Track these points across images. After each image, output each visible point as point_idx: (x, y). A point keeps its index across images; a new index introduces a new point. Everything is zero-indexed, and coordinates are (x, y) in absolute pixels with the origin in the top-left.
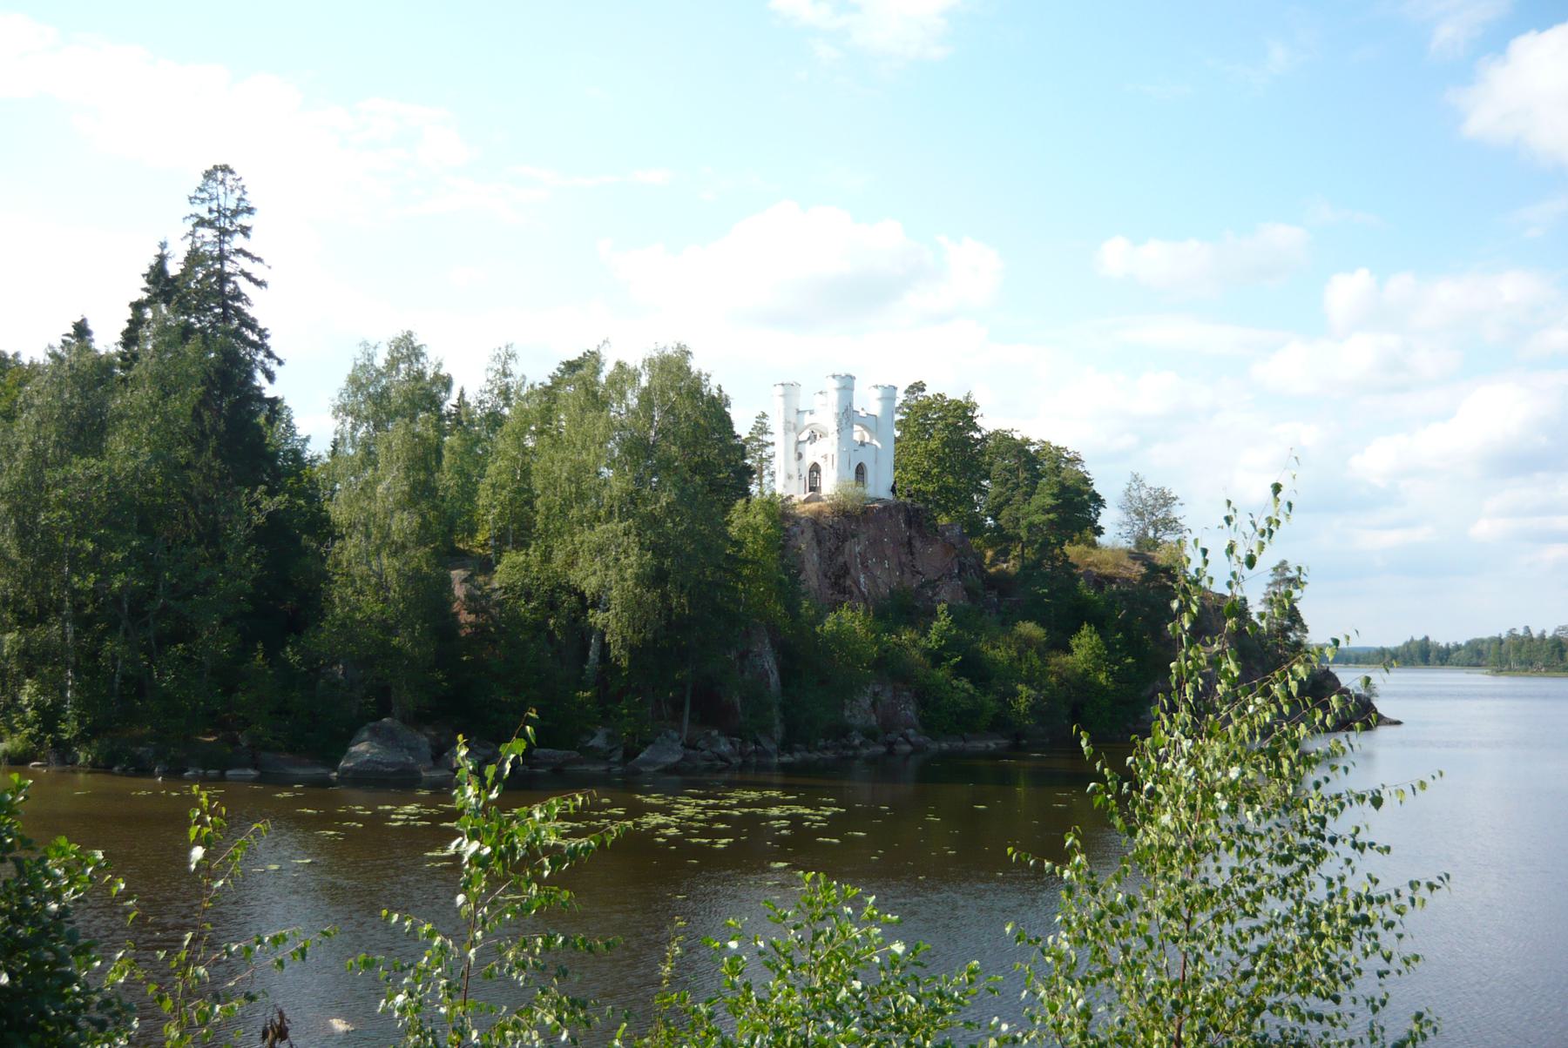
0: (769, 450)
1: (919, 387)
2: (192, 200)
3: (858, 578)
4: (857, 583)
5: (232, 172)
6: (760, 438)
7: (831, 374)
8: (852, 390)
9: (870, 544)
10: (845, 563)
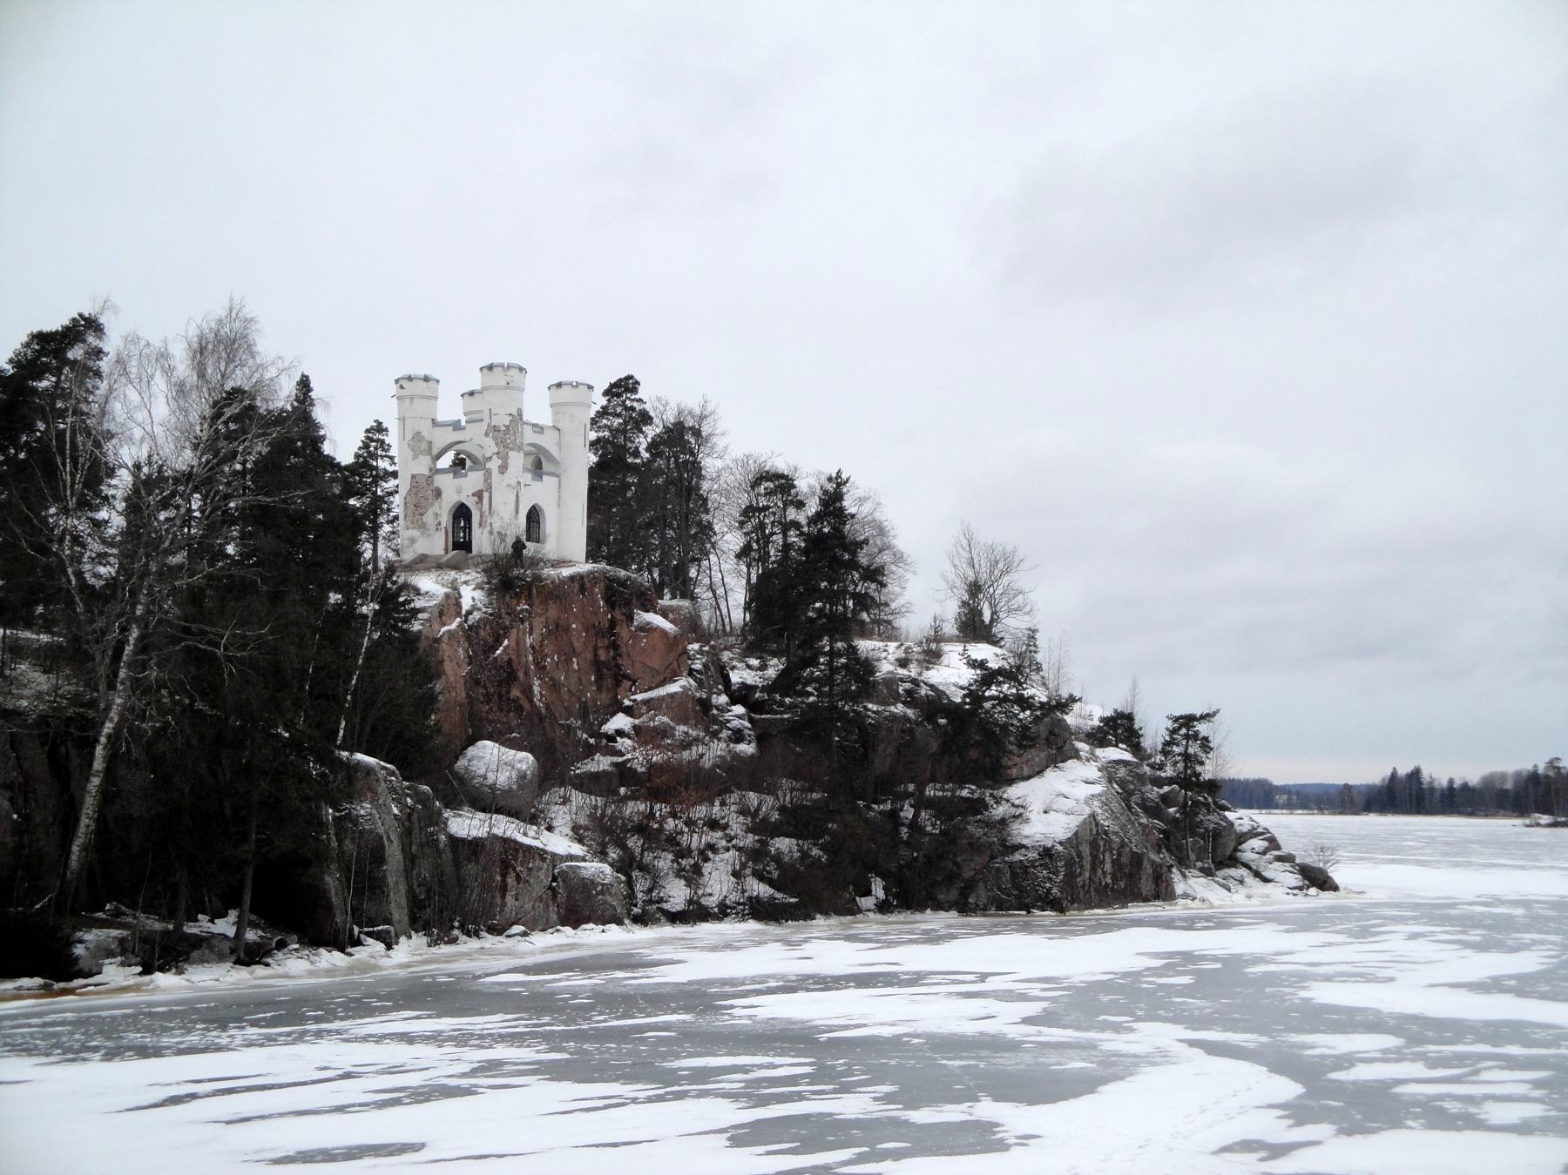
0: (390, 484)
1: (624, 387)
3: (531, 687)
4: (528, 691)
6: (375, 463)
7: (488, 363)
8: (523, 390)
9: (549, 632)
10: (510, 660)
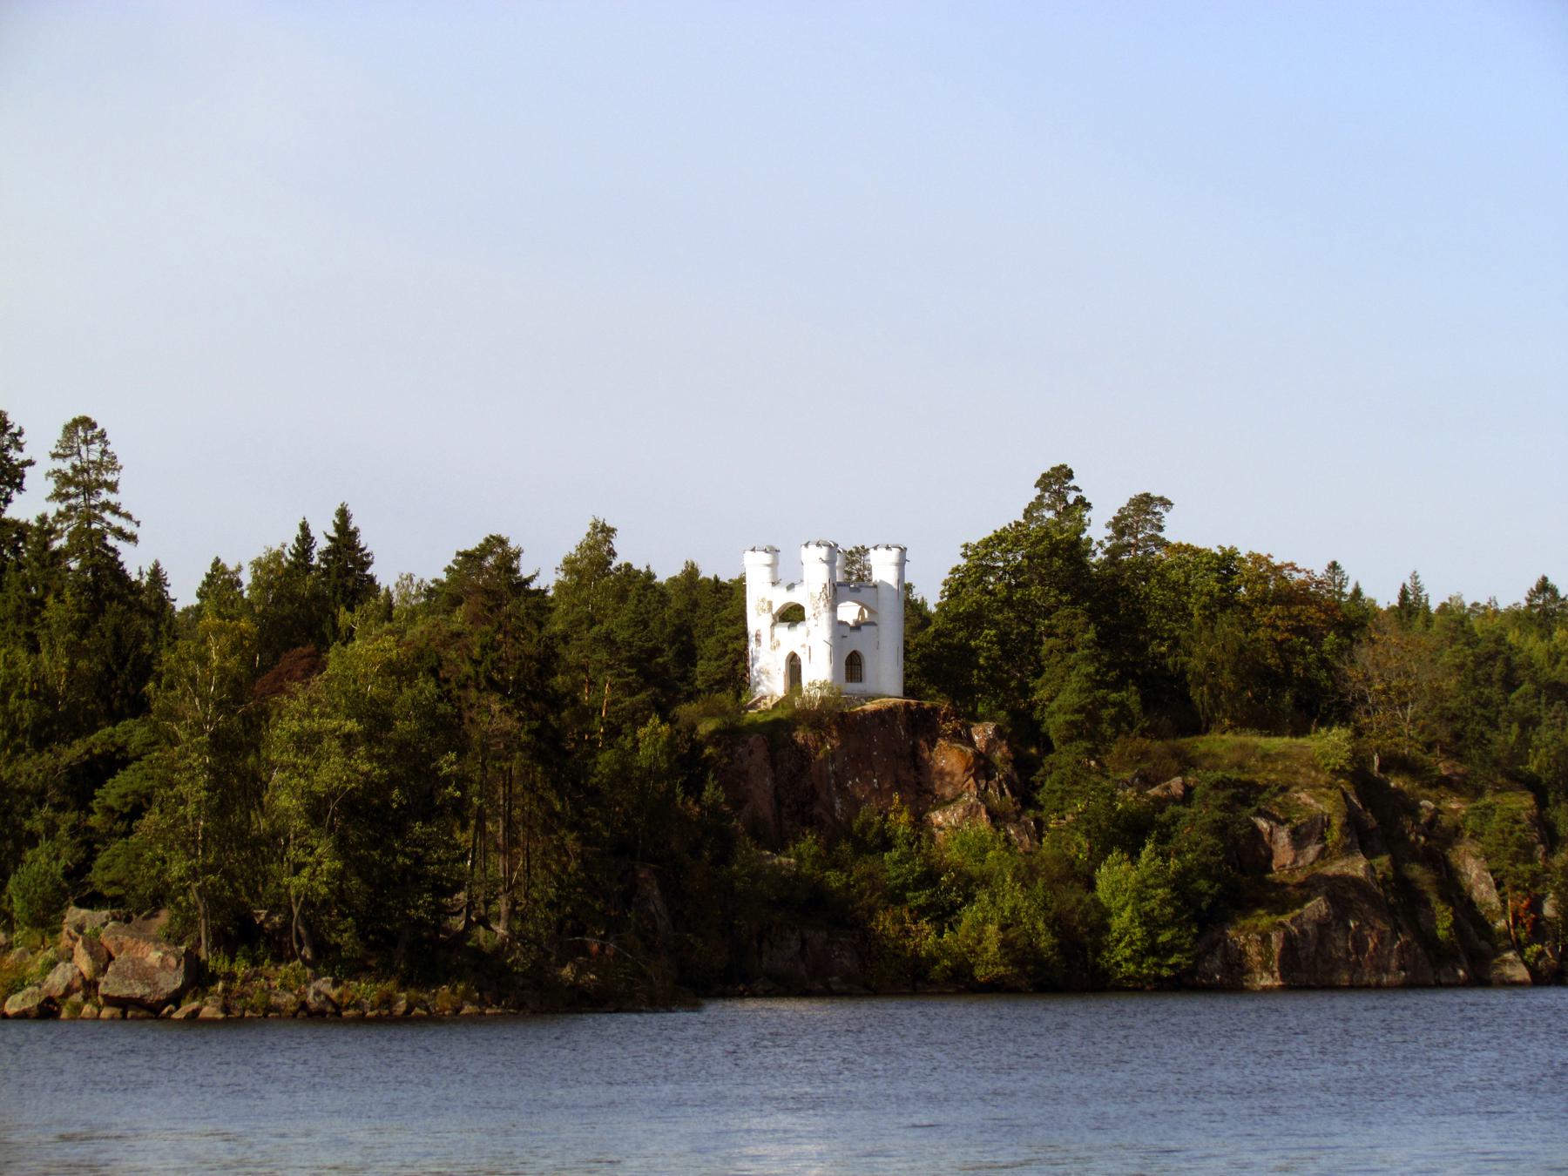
2: (54, 456)
3: (833, 807)
5: (94, 426)
